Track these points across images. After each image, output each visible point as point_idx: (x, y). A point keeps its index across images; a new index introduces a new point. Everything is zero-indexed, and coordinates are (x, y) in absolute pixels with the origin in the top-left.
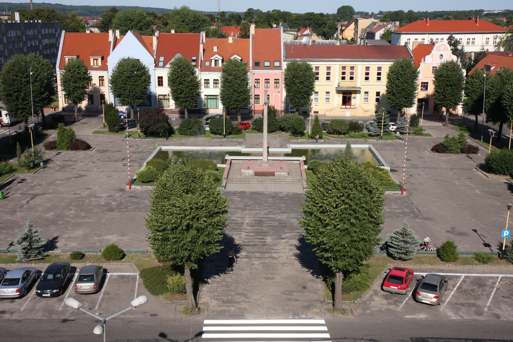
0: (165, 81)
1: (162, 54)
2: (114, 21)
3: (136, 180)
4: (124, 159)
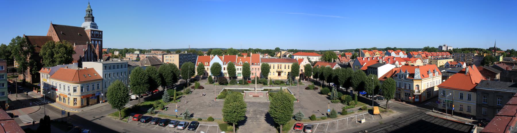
0: (226, 69)
1: (225, 61)
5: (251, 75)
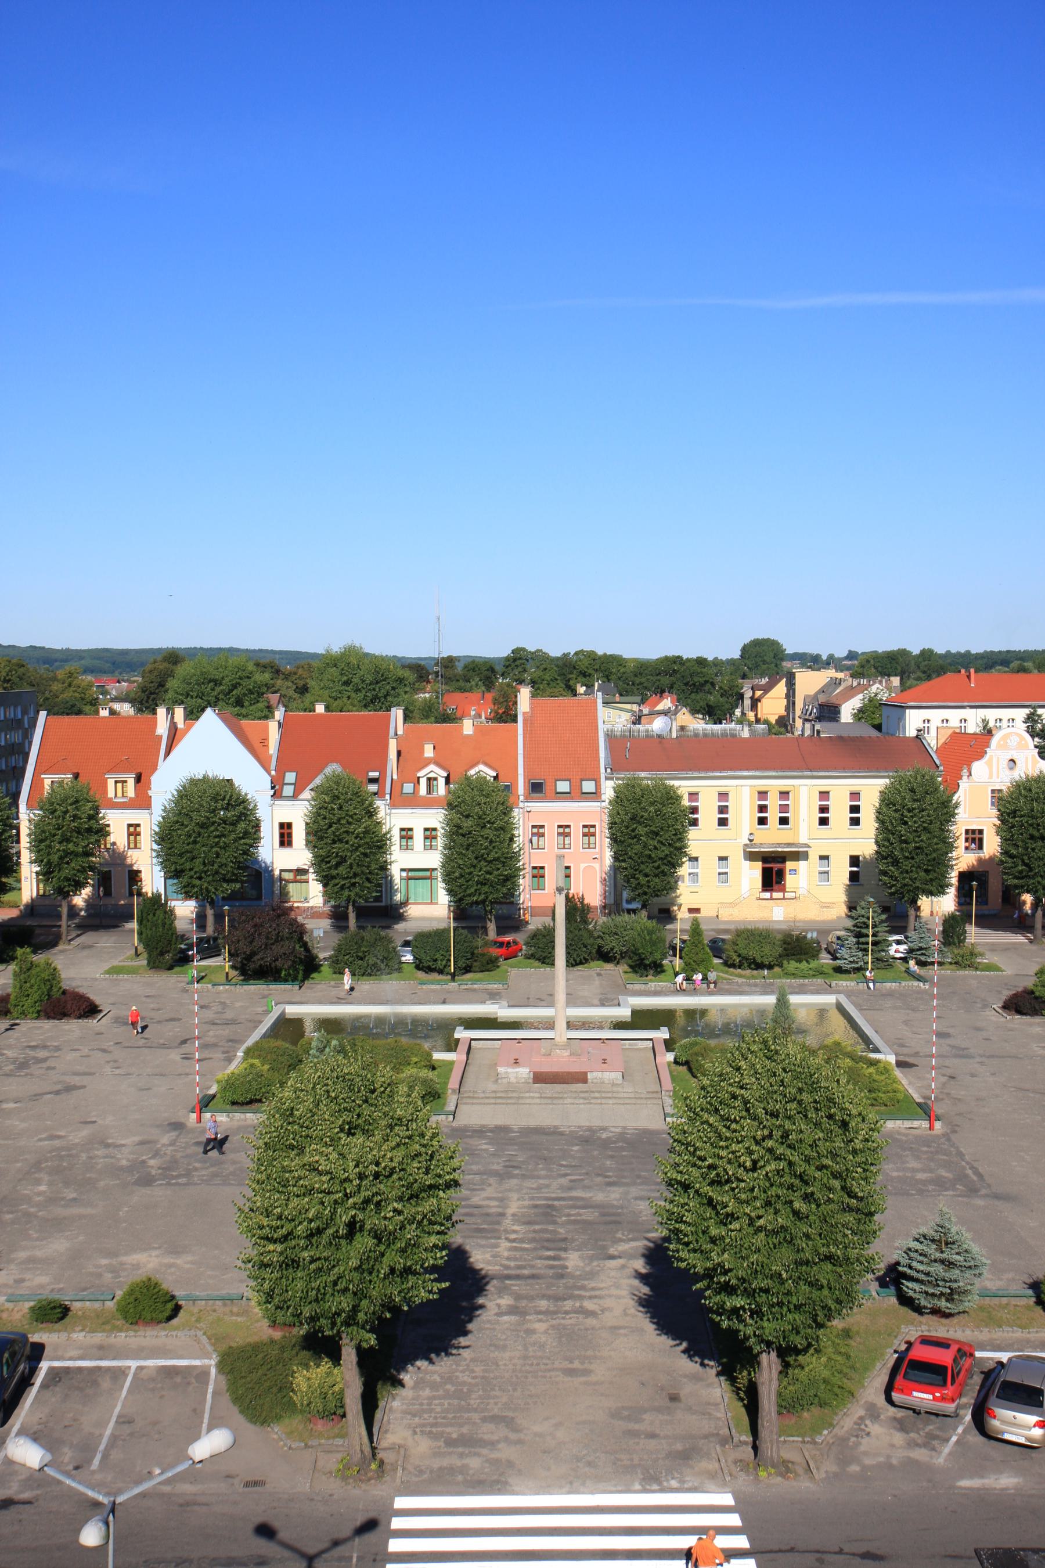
0: (299, 834)
2: (172, 684)
3: (214, 1096)
4: (184, 1042)
5: (524, 882)
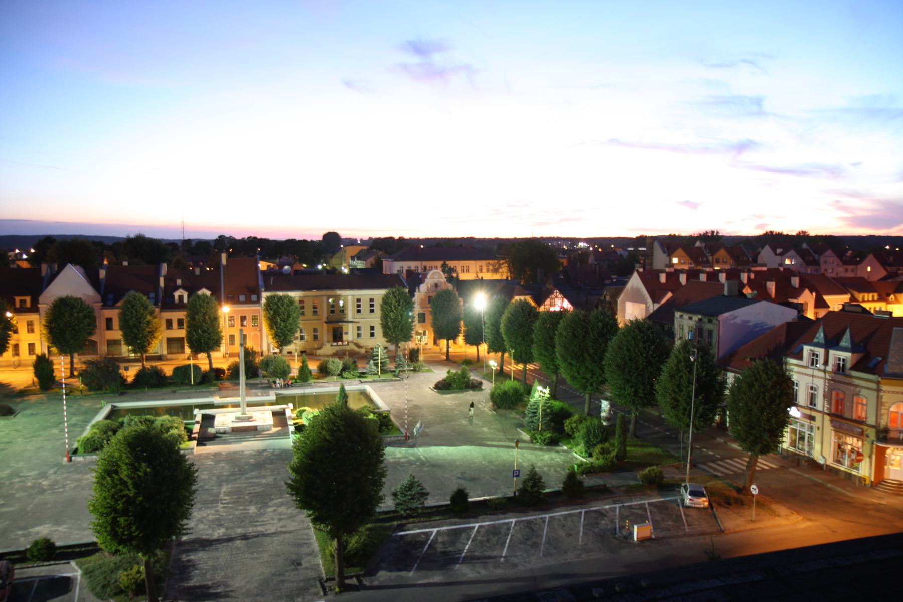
0: (116, 323)
4: (60, 424)
